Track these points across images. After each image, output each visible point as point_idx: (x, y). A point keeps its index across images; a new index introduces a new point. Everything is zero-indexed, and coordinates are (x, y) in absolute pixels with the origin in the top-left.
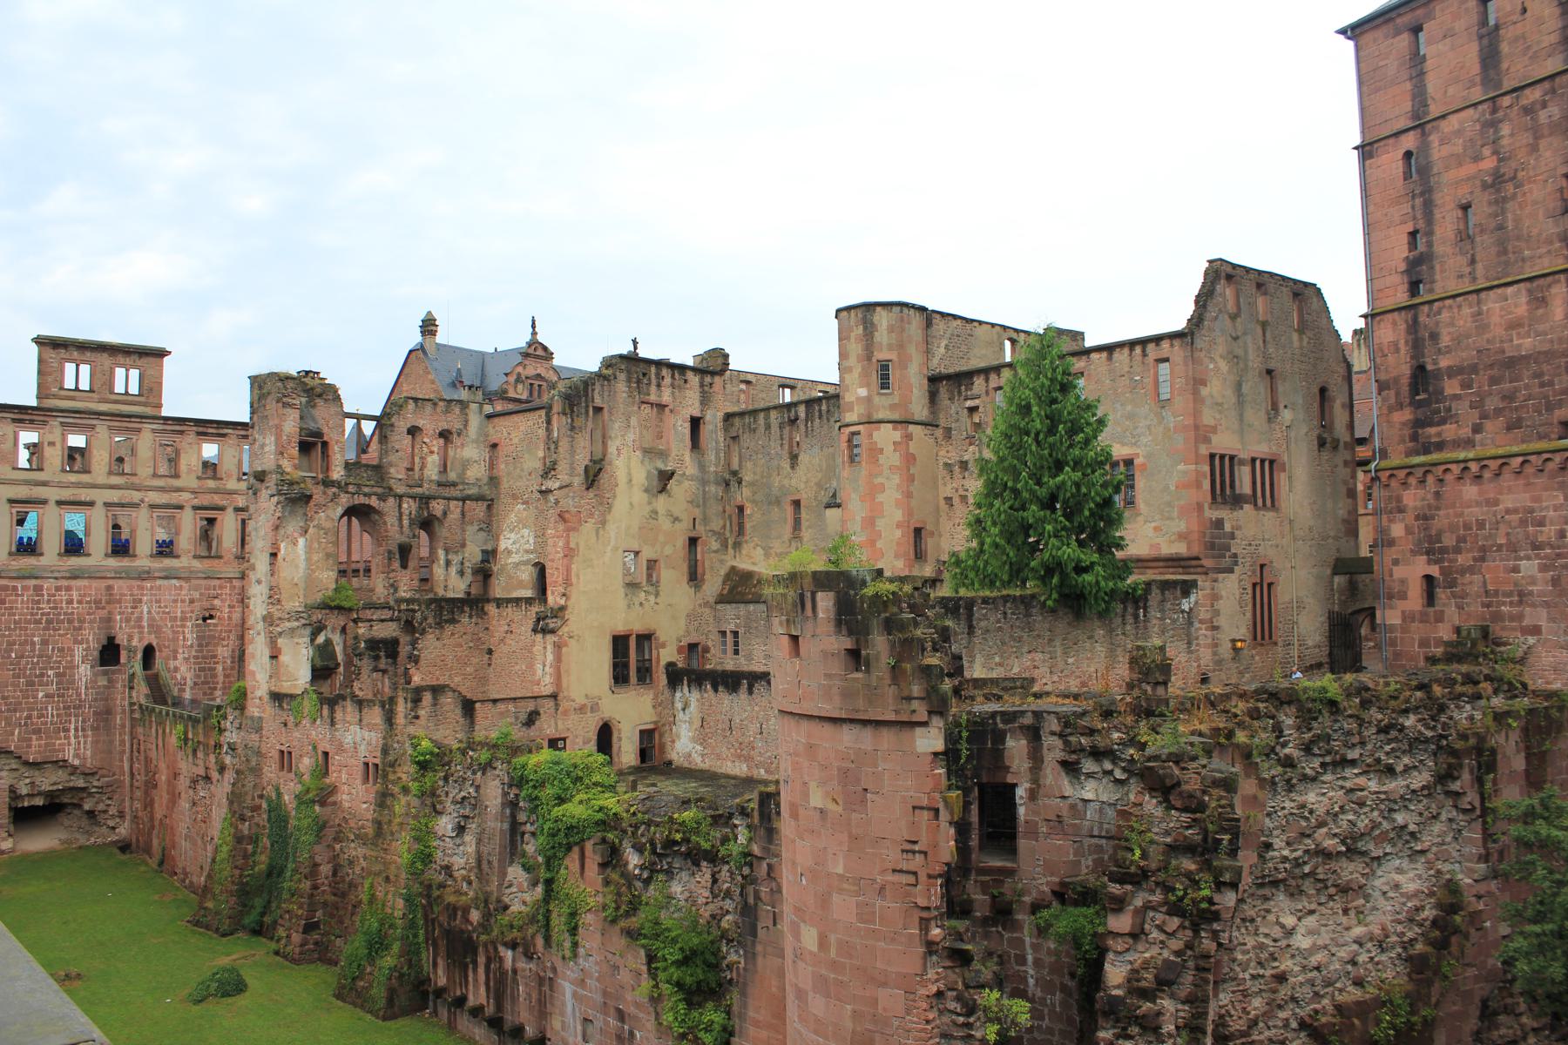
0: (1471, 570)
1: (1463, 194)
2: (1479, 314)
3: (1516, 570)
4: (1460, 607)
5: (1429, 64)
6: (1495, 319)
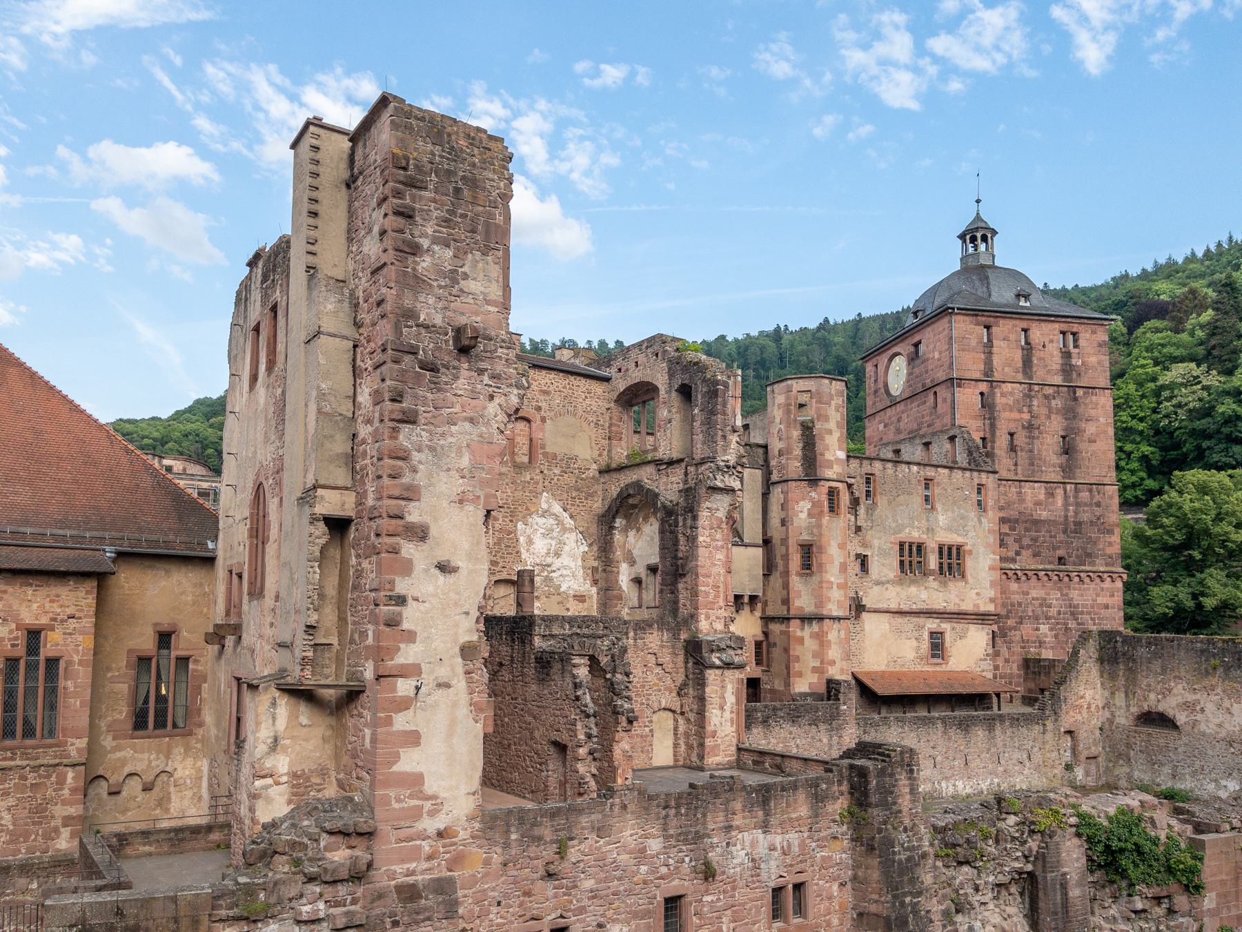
0: (1015, 629)
3: (1038, 629)
5: (995, 350)
6: (1029, 498)
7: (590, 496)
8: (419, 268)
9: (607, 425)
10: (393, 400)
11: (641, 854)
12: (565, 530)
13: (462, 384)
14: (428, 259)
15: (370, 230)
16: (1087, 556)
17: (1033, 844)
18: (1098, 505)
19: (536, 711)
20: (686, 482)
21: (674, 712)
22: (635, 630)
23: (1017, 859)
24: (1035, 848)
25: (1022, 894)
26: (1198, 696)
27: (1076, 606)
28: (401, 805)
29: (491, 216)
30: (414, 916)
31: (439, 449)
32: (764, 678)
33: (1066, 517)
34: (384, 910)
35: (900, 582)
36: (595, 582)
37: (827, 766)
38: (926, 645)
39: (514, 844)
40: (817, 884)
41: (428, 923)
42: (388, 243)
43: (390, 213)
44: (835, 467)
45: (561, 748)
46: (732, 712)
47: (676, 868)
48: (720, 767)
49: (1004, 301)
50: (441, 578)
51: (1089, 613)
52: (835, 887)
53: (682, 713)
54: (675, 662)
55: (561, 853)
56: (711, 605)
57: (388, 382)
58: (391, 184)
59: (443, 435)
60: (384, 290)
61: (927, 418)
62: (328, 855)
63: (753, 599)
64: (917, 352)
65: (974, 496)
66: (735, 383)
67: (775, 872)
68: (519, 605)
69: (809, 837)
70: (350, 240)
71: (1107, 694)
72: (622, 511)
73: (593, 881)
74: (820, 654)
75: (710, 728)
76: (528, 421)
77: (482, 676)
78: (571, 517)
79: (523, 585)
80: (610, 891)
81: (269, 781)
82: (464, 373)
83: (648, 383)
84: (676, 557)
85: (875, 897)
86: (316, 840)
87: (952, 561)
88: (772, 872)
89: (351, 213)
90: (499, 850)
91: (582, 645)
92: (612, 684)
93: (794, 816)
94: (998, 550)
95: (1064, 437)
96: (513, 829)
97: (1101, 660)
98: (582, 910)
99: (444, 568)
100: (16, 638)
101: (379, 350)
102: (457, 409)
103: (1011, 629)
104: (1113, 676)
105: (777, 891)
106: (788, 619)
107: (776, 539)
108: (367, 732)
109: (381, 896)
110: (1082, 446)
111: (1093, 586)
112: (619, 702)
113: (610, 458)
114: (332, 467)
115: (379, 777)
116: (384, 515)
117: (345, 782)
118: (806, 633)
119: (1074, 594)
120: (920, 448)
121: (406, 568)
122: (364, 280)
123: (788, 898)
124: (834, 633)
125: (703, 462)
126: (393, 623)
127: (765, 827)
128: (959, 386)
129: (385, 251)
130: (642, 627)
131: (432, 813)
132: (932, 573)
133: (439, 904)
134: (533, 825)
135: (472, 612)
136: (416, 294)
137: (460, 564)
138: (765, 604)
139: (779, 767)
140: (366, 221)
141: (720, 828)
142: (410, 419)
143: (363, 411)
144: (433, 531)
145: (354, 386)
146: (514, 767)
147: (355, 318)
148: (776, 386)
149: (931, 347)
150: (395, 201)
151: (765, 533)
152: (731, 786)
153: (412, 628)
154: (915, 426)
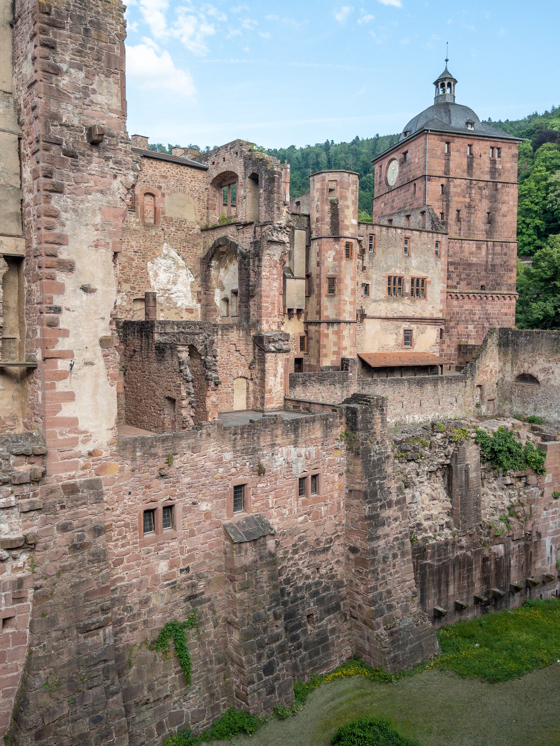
0: (454, 327)
1: (459, 206)
2: (462, 247)
3: (467, 328)
4: (450, 339)
5: (451, 158)
6: (466, 250)
7: (195, 246)
9: (206, 199)
10: (45, 176)
11: (219, 462)
12: (179, 267)
13: (94, 167)
14: (67, 78)
15: (26, 57)
16: (498, 285)
17: (451, 449)
18: (505, 254)
19: (157, 379)
20: (255, 237)
21: (246, 378)
22: (222, 330)
23: (441, 457)
24: (452, 451)
25: (443, 476)
26: (551, 365)
27: (489, 314)
29: (111, 49)
30: (75, 502)
31: (79, 210)
32: (305, 358)
33: (487, 261)
34: (55, 500)
35: (388, 300)
36: (199, 301)
37: (334, 408)
38: (401, 338)
39: (138, 459)
40: (326, 475)
41: (85, 506)
42: (38, 66)
43: (39, 45)
44: (350, 229)
45: (172, 401)
46: (281, 378)
47: (241, 469)
48: (273, 410)
49: (458, 126)
51: (496, 318)
52: (336, 476)
53: (252, 379)
54: (248, 350)
55: (169, 462)
56: (269, 315)
57: (42, 164)
58: (38, 24)
59: (82, 201)
60: (36, 99)
61: (409, 200)
62: (16, 468)
63: (299, 311)
64: (405, 158)
65: (434, 249)
66: (286, 173)
67: (301, 469)
68: (147, 314)
69: (322, 449)
70: (14, 64)
71: (501, 364)
72: (215, 256)
73: (189, 478)
74: (337, 344)
75: (268, 388)
76: (153, 195)
77: (115, 358)
78: (183, 259)
79: (149, 302)
80: (200, 484)
82: (95, 159)
83: (232, 173)
84: (248, 285)
85: (359, 481)
86: (7, 460)
87: (419, 287)
88: (299, 469)
89: (14, 45)
90: (129, 462)
91: (186, 339)
92: (205, 362)
93: (312, 437)
94: (446, 281)
95: (488, 213)
96: (138, 450)
97: (499, 345)
98: (183, 495)
99: (86, 289)
101: (34, 142)
102: (92, 184)
103: (452, 328)
104: (505, 354)
105: (302, 480)
106: (320, 323)
107: (314, 275)
108: (40, 393)
109: (52, 491)
110: (499, 218)
111: (499, 302)
112: (210, 373)
113: (208, 221)
114: (7, 222)
115: (48, 421)
116: (43, 254)
117: (28, 424)
118: (330, 331)
119: (489, 307)
120: (404, 218)
121: (61, 289)
122: (23, 92)
124: (347, 331)
125: (265, 224)
126: (52, 324)
127: (295, 444)
128: (429, 180)
129: (36, 71)
130: (226, 328)
132: (407, 295)
133: (90, 495)
134: (151, 447)
135: (106, 318)
136: (59, 102)
137: (97, 287)
138: (307, 314)
139: (308, 409)
140: (24, 51)
141: (268, 445)
142: (58, 190)
143: (27, 184)
144: (78, 266)
145: (20, 166)
146: (144, 413)
147: (18, 119)
148: (315, 177)
149: (413, 155)
150: (42, 36)
151: (307, 270)
152: (275, 421)
154: (402, 205)
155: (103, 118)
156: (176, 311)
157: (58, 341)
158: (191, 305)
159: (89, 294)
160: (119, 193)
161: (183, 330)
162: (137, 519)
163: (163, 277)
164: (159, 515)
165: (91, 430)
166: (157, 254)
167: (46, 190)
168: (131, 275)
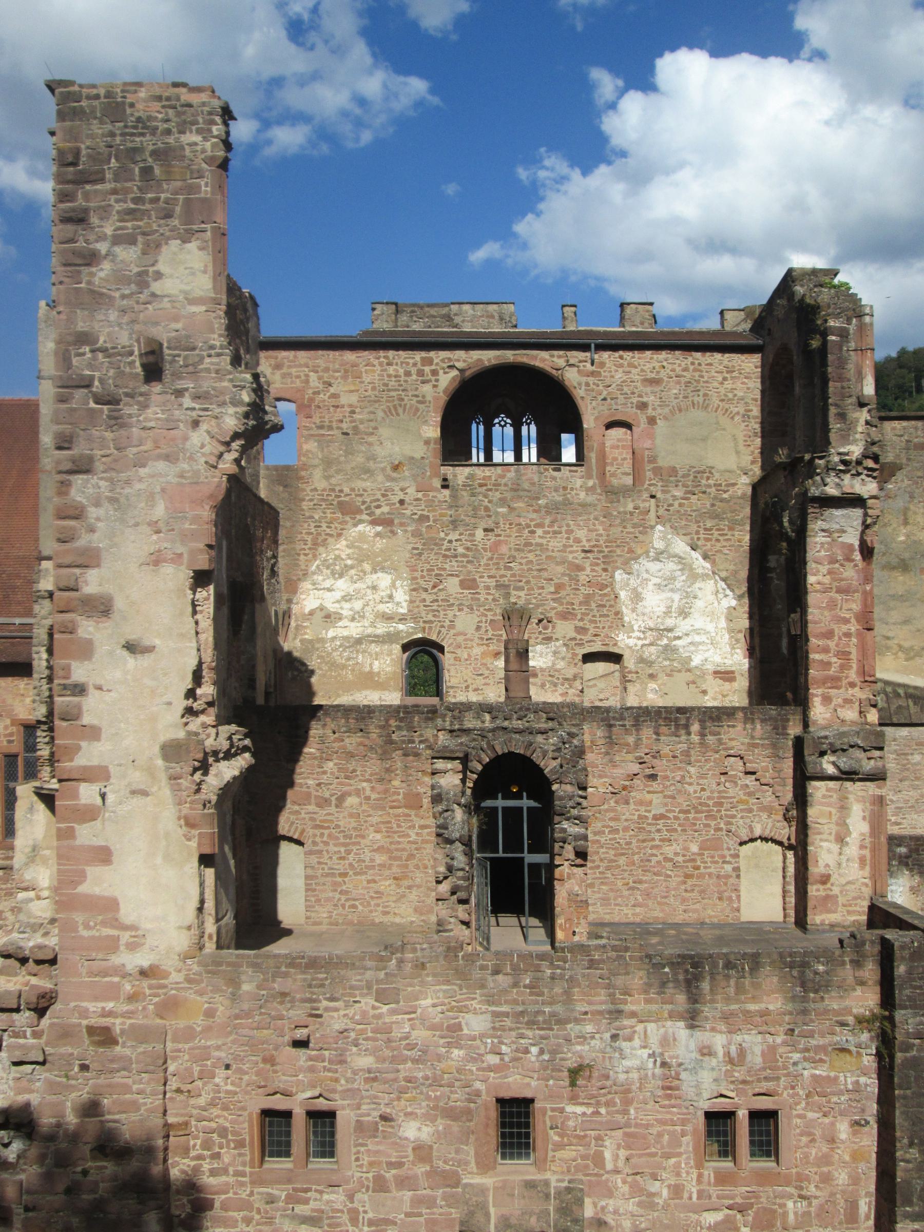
8: (96, 280)
10: (59, 448)
12: (694, 577)
28: (94, 933)
31: (122, 500)
50: (131, 662)
59: (128, 482)
78: (705, 557)
81: (32, 894)
99: (131, 648)
100: (11, 734)
123: (743, 1132)
131: (133, 947)
137: (157, 642)
144: (119, 603)
153: (95, 722)
155: (176, 319)
156: (689, 677)
157: (79, 748)
158: (728, 662)
159: (139, 656)
160: (204, 455)
161: (506, 724)
162: (247, 1127)
163: (655, 602)
164: (299, 1126)
165: (146, 925)
166: (639, 551)
167: (60, 472)
168: (576, 602)
